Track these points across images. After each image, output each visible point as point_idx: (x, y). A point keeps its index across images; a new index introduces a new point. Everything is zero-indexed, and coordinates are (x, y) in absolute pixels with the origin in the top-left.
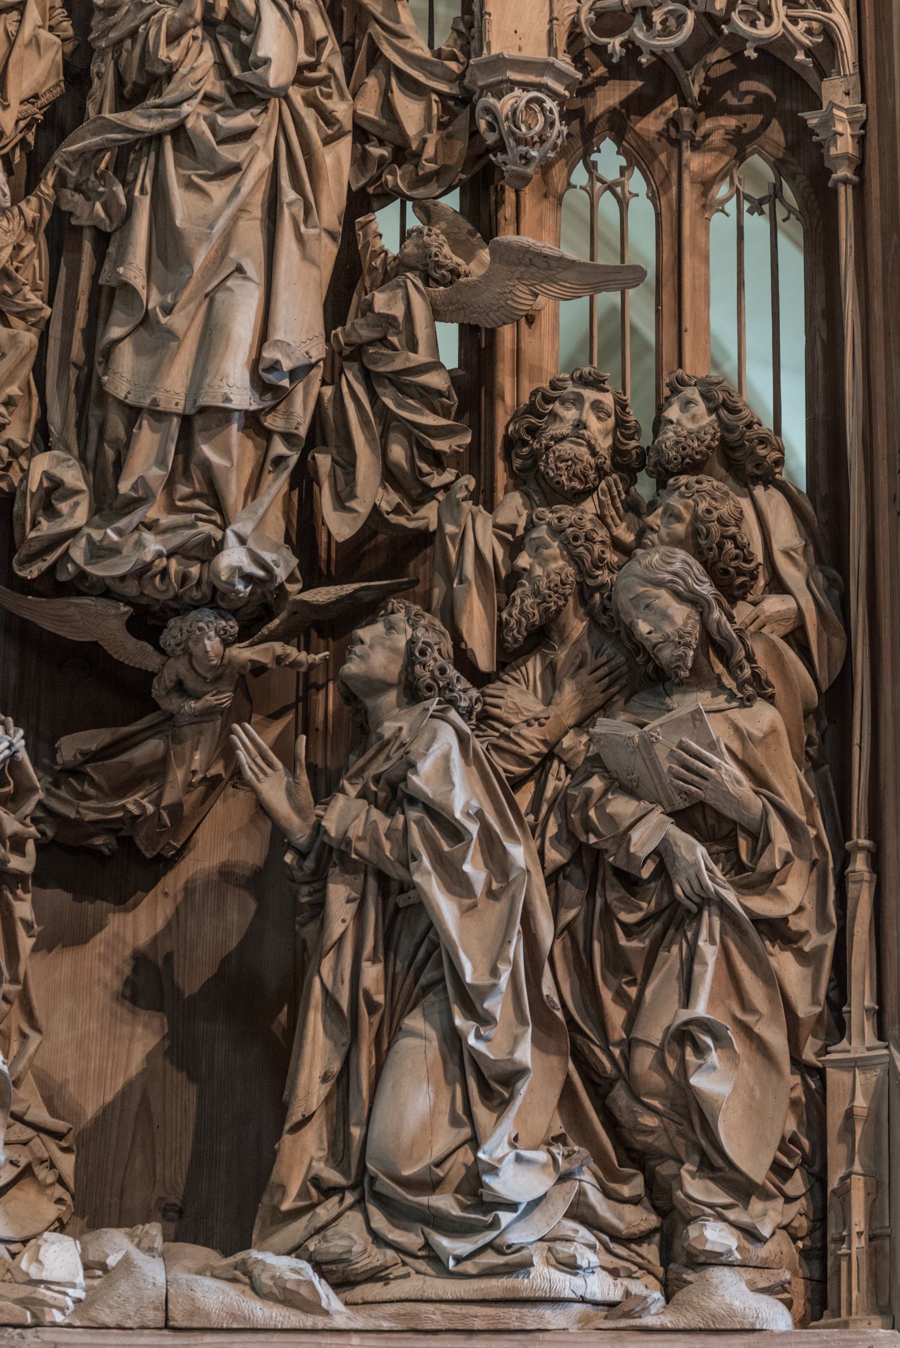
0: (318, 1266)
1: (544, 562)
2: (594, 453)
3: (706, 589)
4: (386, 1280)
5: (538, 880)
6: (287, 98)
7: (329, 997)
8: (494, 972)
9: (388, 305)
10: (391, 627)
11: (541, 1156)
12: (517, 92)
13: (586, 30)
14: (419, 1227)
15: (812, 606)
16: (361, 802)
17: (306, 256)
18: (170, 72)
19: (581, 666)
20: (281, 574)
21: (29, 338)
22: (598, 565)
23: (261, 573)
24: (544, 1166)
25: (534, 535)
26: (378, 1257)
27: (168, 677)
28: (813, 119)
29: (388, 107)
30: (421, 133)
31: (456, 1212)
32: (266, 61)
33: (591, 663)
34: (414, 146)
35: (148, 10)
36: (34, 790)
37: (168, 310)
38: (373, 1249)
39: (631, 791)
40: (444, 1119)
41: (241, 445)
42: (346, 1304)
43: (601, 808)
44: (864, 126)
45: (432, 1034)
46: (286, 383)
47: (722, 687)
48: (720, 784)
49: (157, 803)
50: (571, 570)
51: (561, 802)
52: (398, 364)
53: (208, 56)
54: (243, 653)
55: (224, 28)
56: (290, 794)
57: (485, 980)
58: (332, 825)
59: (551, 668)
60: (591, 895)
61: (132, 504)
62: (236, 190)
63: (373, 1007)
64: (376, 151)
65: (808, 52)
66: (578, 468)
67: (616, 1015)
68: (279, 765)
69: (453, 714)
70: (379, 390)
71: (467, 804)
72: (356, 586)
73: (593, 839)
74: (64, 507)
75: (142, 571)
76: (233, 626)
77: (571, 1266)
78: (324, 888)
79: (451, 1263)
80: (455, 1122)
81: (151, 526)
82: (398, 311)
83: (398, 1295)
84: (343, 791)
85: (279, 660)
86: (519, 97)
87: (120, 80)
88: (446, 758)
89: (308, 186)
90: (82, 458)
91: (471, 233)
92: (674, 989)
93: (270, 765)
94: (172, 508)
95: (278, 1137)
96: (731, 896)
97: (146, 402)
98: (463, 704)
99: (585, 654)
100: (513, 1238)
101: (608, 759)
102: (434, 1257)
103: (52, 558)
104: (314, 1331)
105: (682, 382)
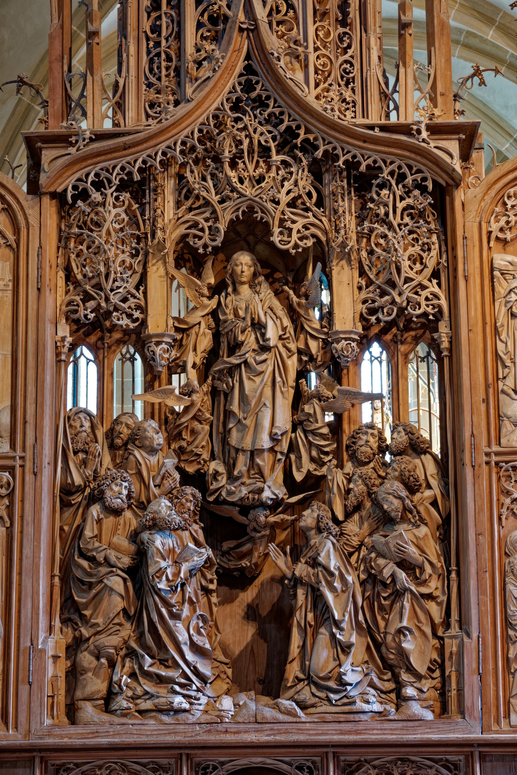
0: (298, 703)
1: (357, 486)
2: (372, 449)
3: (404, 493)
4: (316, 707)
5: (357, 584)
6: (277, 347)
7: (298, 623)
8: (344, 615)
9: (309, 409)
10: (313, 511)
11: (359, 669)
12: (343, 341)
13: (365, 315)
14: (325, 691)
15: (439, 493)
16: (305, 565)
17: (284, 397)
18: (242, 343)
19: (369, 517)
20: (280, 496)
21: (207, 428)
22: (374, 485)
23: (275, 497)
24: (360, 672)
25: (354, 478)
26: (314, 700)
27: (251, 527)
28: (436, 336)
29: (307, 344)
30: (317, 353)
31: (335, 687)
32: (269, 339)
33: (372, 516)
34: (315, 357)
35: (235, 323)
36: (215, 564)
37: (245, 419)
38: (312, 698)
39: (384, 557)
40: (332, 659)
41: (269, 457)
42: (306, 714)
43: (375, 561)
44: (451, 338)
45: (327, 634)
46: (280, 438)
47: (411, 522)
48: (409, 554)
49: (250, 562)
50: (365, 488)
51: (364, 559)
52: (312, 428)
53: (253, 337)
54: (272, 519)
55: (257, 326)
56: (286, 563)
57: (342, 618)
58: (297, 573)
59: (361, 517)
60: (374, 587)
61: (237, 478)
62: (263, 380)
63: (311, 626)
64: (305, 358)
65: (433, 315)
66: (367, 455)
67: (382, 624)
68: (282, 554)
69: (331, 537)
70: (308, 435)
71: (335, 565)
72: (304, 495)
73: (373, 572)
74: (219, 478)
75: (242, 499)
76: (268, 512)
77: (368, 702)
78: (296, 590)
79: (334, 702)
80: (334, 660)
81: (243, 484)
82: (312, 412)
83: (319, 711)
84: (300, 562)
85: (282, 520)
86: (344, 343)
87: (229, 343)
88: (329, 551)
89: (284, 375)
90: (224, 462)
91: (334, 382)
92: (398, 616)
93: (280, 555)
94: (249, 478)
95: (285, 665)
96: (413, 588)
97: (240, 447)
98: (334, 533)
99: (370, 513)
100: (351, 694)
101: (376, 547)
102: (329, 700)
103: (217, 494)
104: (296, 722)
105: (398, 426)
